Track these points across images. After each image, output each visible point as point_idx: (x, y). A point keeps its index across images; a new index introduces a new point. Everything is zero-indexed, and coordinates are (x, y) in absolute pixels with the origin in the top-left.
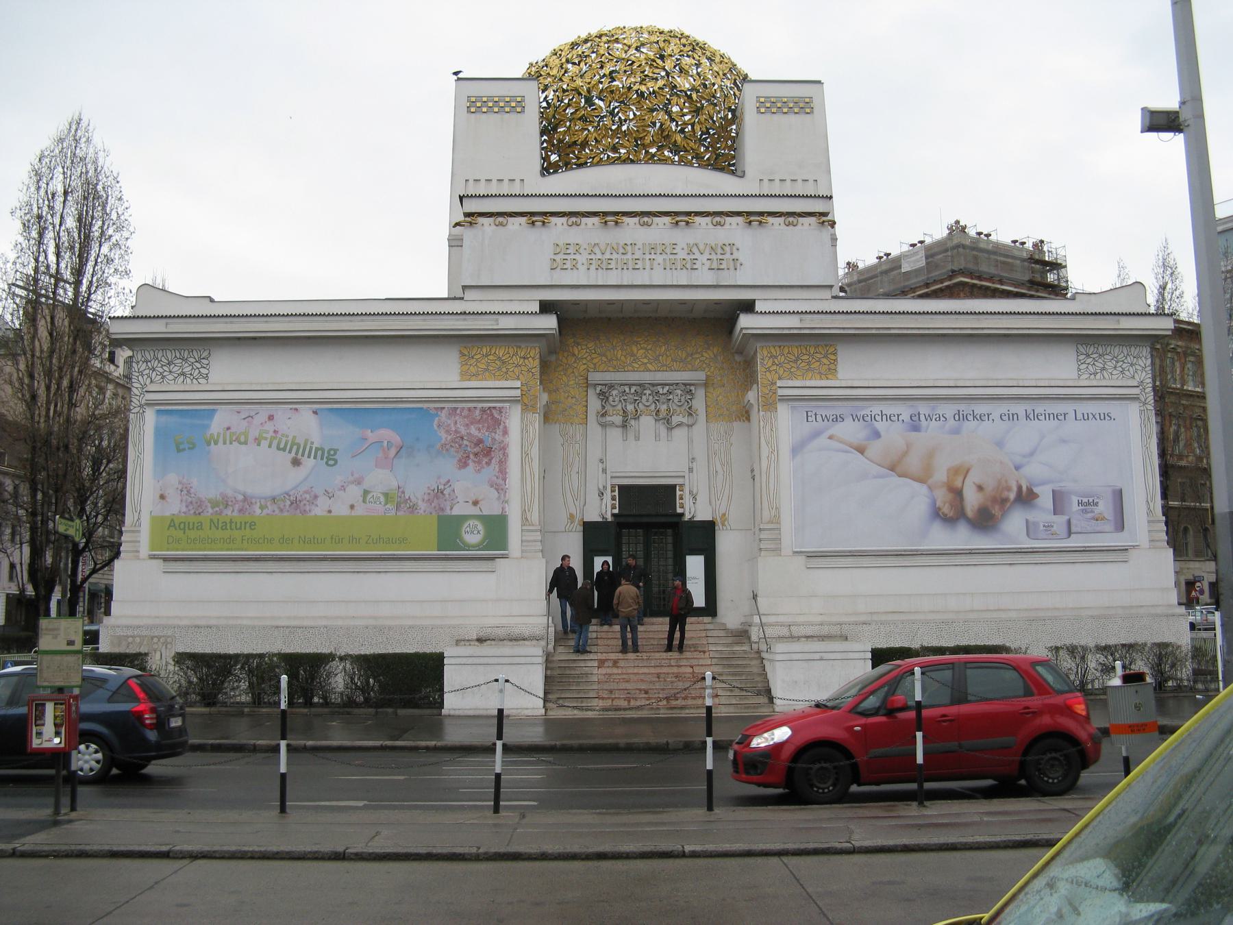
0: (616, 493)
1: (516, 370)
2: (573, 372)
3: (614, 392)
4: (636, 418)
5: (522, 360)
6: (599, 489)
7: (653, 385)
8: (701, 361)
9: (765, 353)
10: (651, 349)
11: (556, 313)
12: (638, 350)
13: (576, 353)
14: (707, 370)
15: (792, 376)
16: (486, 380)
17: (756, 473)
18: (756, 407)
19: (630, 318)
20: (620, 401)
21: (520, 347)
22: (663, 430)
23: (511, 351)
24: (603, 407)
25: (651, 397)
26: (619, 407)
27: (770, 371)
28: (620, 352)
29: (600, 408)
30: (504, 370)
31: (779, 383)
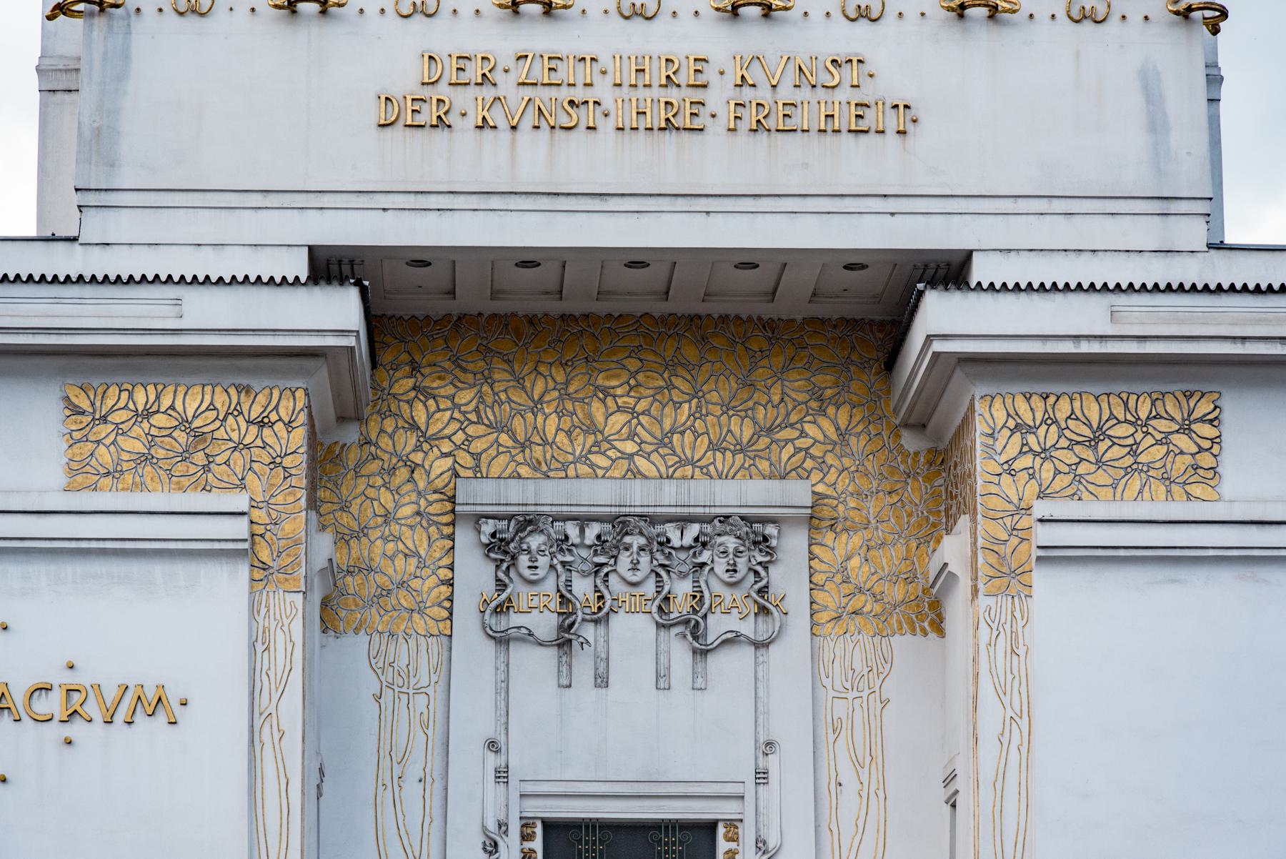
0: (537, 844)
1: (238, 460)
2: (411, 480)
3: (535, 541)
4: (600, 619)
5: (254, 429)
6: (484, 829)
8: (798, 450)
9: (1000, 416)
10: (646, 412)
11: (358, 283)
13: (420, 416)
14: (816, 476)
15: (1078, 485)
16: (140, 486)
18: (964, 583)
19: (586, 316)
20: (552, 567)
21: (248, 390)
22: (679, 652)
23: (221, 400)
26: (549, 586)
27: (1012, 473)
28: (553, 422)
29: (492, 585)
30: (200, 458)
31: (1042, 508)
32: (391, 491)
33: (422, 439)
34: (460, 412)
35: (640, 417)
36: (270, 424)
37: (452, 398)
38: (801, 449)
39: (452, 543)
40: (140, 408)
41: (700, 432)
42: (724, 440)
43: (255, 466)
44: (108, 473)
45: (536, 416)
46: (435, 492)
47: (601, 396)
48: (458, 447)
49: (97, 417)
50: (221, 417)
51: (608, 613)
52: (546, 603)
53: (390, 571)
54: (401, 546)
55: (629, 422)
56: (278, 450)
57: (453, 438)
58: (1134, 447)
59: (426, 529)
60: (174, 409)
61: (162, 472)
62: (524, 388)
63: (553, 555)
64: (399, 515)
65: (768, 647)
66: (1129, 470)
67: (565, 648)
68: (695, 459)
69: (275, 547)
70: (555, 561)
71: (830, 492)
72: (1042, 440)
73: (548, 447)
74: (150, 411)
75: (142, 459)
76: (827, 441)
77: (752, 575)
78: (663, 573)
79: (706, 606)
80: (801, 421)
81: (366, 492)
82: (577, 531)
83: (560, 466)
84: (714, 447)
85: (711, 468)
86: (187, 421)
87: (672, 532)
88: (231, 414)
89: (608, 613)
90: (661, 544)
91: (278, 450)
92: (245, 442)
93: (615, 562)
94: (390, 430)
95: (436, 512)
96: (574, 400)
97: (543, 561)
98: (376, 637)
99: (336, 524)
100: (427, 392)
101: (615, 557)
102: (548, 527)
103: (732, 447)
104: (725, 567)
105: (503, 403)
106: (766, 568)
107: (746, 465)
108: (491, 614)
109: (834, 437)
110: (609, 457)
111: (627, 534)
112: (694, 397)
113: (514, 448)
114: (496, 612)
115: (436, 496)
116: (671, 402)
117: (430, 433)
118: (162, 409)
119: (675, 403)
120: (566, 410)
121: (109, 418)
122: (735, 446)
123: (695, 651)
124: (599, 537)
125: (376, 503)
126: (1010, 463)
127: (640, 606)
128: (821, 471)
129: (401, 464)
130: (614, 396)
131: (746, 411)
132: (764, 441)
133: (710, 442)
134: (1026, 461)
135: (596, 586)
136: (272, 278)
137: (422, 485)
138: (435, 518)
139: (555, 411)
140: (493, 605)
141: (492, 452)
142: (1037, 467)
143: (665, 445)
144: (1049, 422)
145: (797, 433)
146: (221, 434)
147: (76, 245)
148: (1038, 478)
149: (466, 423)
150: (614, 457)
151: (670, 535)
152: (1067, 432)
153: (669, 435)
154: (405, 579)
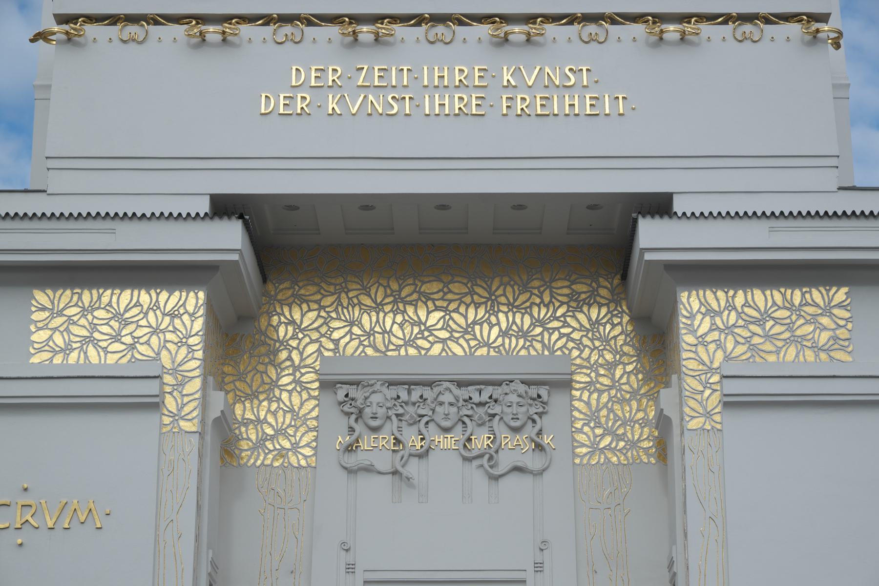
2: (289, 358)
4: (423, 455)
5: (167, 319)
7: (461, 384)
9: (696, 305)
11: (241, 217)
12: (429, 313)
13: (297, 316)
17: (679, 568)
24: (352, 430)
25: (454, 410)
27: (705, 345)
30: (128, 340)
32: (275, 366)
33: (297, 331)
34: (325, 311)
35: (452, 314)
36: (179, 315)
37: (318, 302)
38: (564, 335)
39: (317, 402)
40: (87, 305)
41: (494, 323)
42: (511, 329)
43: (168, 345)
44: (62, 350)
45: (378, 314)
47: (424, 300)
48: (322, 336)
49: (55, 312)
50: (144, 311)
51: (428, 451)
52: (384, 443)
53: (274, 424)
54: (282, 406)
55: (444, 317)
56: (184, 332)
58: (791, 325)
60: (111, 306)
61: (100, 350)
62: (370, 296)
64: (280, 383)
65: (542, 474)
66: (788, 341)
68: (490, 342)
69: (179, 401)
70: (390, 413)
71: (585, 364)
72: (725, 321)
73: (386, 335)
74: (93, 307)
75: (88, 340)
76: (583, 329)
77: (530, 422)
78: (466, 419)
79: (497, 443)
80: (564, 315)
81: (257, 368)
82: (406, 392)
83: (394, 348)
84: (504, 334)
85: (501, 348)
86: (120, 315)
87: (472, 392)
88: (152, 309)
89: (428, 451)
90: (465, 401)
91: (184, 332)
92: (161, 328)
93: (433, 413)
94: (275, 324)
96: (406, 303)
99: (236, 389)
100: (302, 298)
101: (433, 411)
102: (384, 389)
103: (516, 334)
105: (355, 305)
106: (541, 417)
107: (526, 346)
108: (344, 452)
109: (588, 326)
110: (429, 342)
112: (489, 299)
113: (363, 336)
114: (349, 451)
116: (472, 305)
117: (303, 327)
118: (102, 306)
119: (475, 304)
120: (400, 310)
121: (64, 313)
122: (517, 332)
123: (490, 478)
124: (421, 397)
125: (264, 375)
126: (703, 337)
127: (451, 446)
128: (579, 349)
129: (282, 347)
130: (433, 300)
131: (525, 308)
132: (538, 330)
133: (501, 329)
134: (715, 335)
135: (419, 431)
136: (180, 214)
137: (297, 362)
139: (391, 311)
140: (345, 445)
141: (347, 338)
142: (723, 341)
143: (469, 333)
144: (730, 308)
145: (561, 324)
146: (143, 322)
147: (44, 194)
148: (723, 347)
149: (329, 319)
150: (432, 341)
152: (742, 315)
153: (472, 326)
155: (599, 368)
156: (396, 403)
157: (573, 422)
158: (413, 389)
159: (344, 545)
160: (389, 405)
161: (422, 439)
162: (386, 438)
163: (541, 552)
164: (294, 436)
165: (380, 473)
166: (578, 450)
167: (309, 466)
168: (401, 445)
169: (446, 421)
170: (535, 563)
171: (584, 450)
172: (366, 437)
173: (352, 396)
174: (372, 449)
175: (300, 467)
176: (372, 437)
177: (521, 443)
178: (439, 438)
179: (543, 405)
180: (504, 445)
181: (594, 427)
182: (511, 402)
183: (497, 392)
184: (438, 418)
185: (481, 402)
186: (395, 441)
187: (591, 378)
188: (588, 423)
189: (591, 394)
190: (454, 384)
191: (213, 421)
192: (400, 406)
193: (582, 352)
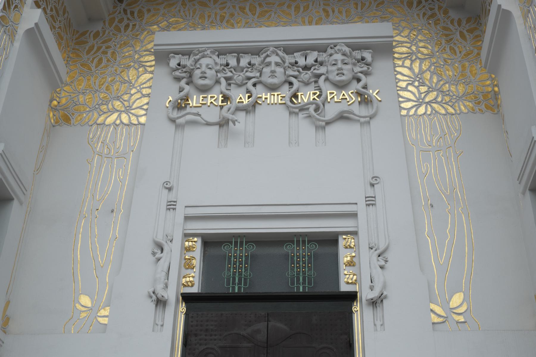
3: (204, 62)
7: (289, 50)
46: (145, 51)
52: (212, 100)
57: (160, 25)
59: (137, 69)
63: (217, 72)
65: (369, 123)
67: (225, 127)
77: (355, 82)
79: (323, 96)
90: (290, 64)
95: (144, 61)
97: (210, 73)
98: (94, 127)
104: (336, 72)
108: (173, 109)
111: (268, 56)
115: (148, 53)
123: (317, 128)
124: (250, 64)
138: (144, 64)
151: (296, 60)
154: (119, 95)
155: (419, 42)
156: (225, 68)
157: (397, 83)
158: (242, 57)
159: (167, 184)
160: (218, 67)
161: (249, 97)
162: (214, 97)
163: (372, 188)
164: (128, 101)
165: (208, 124)
166: (403, 105)
167: (140, 124)
168: (229, 103)
169: (273, 78)
170: (366, 198)
171: (409, 105)
172: (195, 97)
173: (183, 63)
174: (201, 105)
175: (130, 124)
176: (201, 96)
177: (347, 97)
178: (266, 95)
179: (368, 66)
180: (330, 99)
181: (419, 86)
182: (336, 60)
183: (323, 57)
184: (264, 79)
185: (307, 64)
186: (223, 99)
187: (411, 50)
188: (412, 83)
189: (412, 61)
190: (280, 50)
191: (26, 31)
192: (229, 71)
193: (402, 31)
